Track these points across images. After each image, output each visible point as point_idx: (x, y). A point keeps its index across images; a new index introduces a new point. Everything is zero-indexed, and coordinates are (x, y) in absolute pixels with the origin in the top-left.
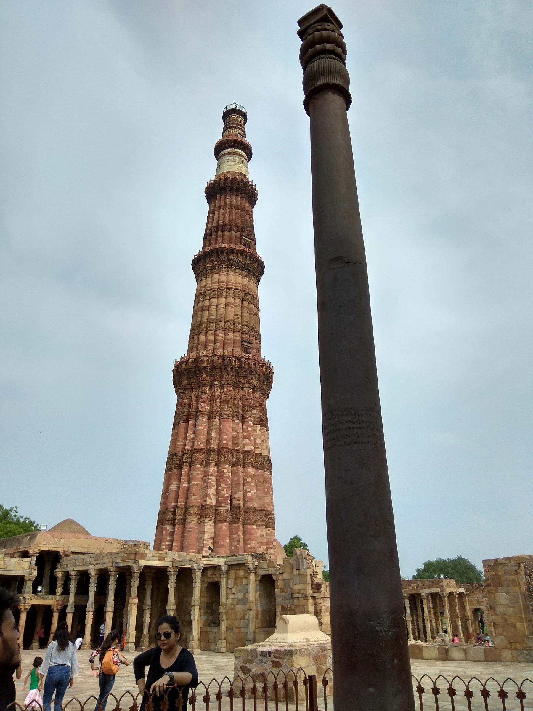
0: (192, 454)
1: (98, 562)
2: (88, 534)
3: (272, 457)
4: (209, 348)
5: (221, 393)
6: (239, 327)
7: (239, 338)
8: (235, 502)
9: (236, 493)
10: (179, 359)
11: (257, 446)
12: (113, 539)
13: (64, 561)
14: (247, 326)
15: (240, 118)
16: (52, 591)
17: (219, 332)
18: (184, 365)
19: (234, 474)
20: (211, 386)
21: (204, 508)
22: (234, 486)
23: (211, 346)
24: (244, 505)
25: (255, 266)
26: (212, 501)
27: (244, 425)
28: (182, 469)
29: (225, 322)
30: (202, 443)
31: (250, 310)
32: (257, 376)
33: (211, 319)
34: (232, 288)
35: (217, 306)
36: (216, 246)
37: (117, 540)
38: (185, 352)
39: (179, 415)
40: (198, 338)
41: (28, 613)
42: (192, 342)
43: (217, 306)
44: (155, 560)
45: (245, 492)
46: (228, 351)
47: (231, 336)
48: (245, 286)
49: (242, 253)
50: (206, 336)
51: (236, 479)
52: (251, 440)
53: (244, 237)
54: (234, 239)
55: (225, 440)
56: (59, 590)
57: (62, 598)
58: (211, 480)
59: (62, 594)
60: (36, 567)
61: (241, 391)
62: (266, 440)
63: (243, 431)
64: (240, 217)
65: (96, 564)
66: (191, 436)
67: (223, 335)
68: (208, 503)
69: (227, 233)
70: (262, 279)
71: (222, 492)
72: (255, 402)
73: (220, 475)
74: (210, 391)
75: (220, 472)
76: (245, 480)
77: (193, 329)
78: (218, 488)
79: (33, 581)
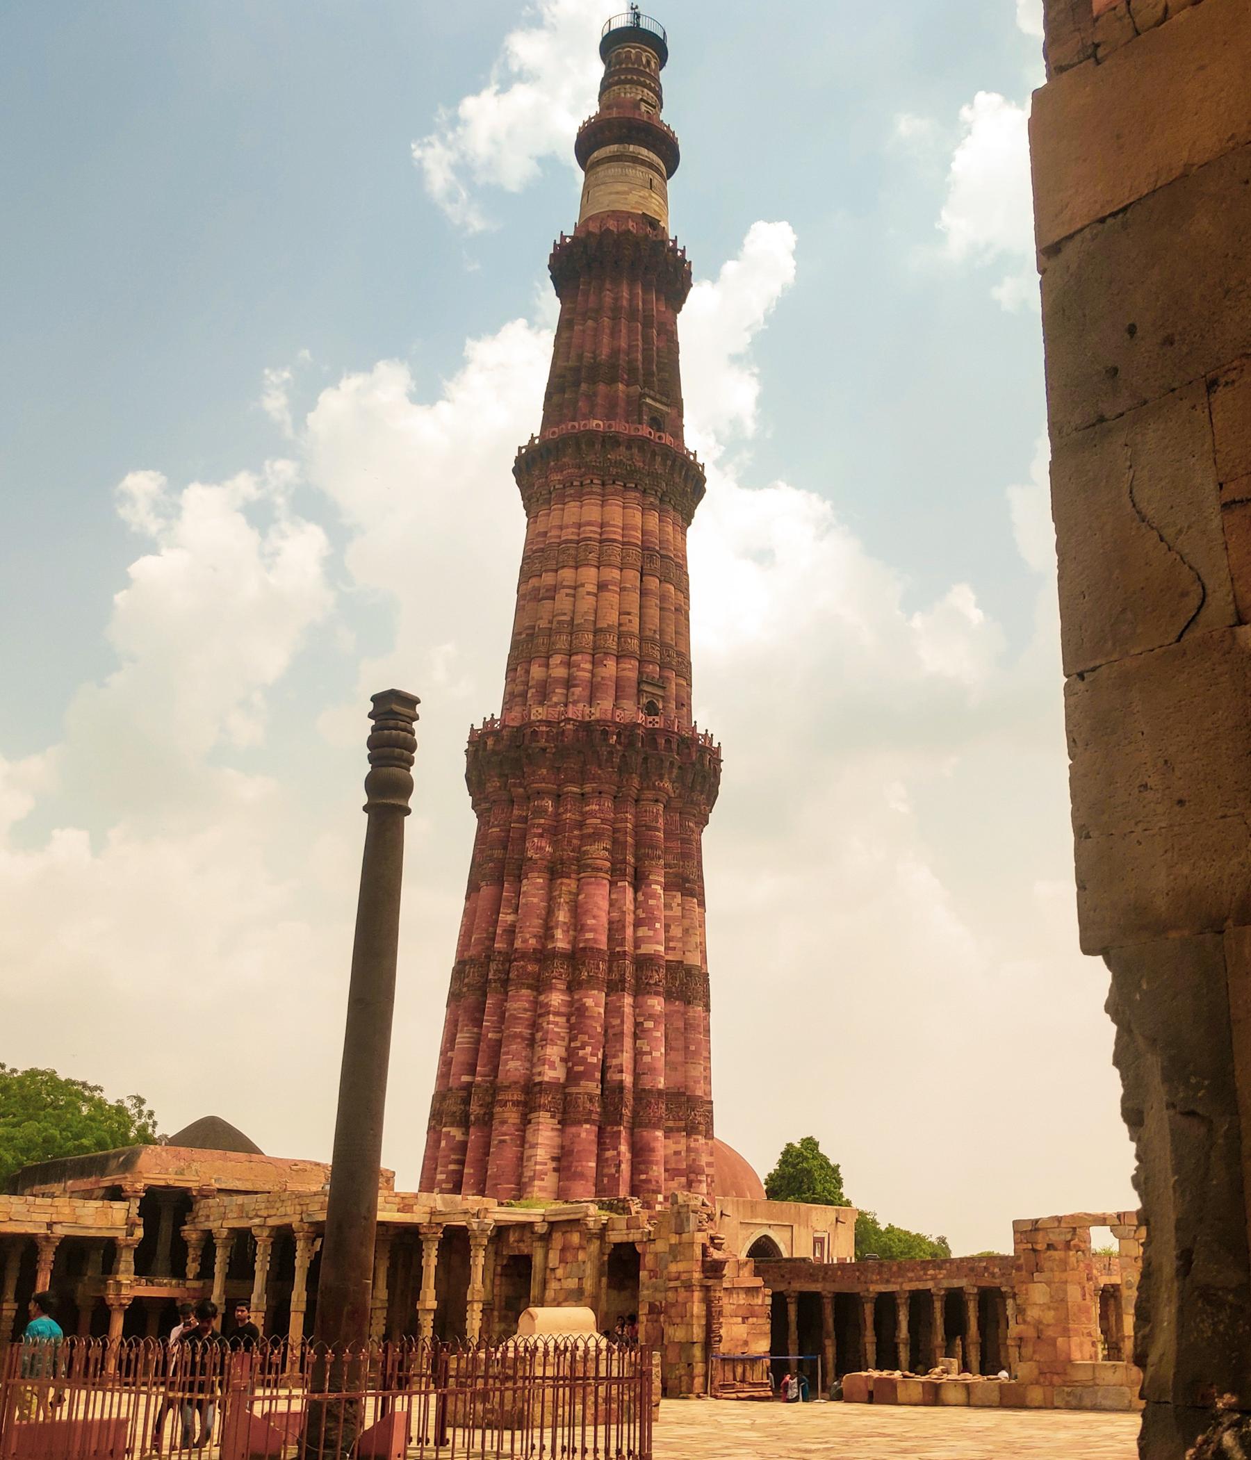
0: (511, 962)
1: (272, 1212)
2: (257, 1151)
3: (712, 969)
4: (555, 699)
5: (583, 814)
6: (634, 644)
7: (634, 675)
8: (613, 1076)
9: (615, 1056)
10: (479, 726)
11: (671, 944)
12: (311, 1163)
13: (202, 1207)
14: (653, 640)
15: (648, 54)
16: (178, 1272)
17: (579, 657)
18: (490, 742)
19: (612, 1010)
20: (558, 798)
21: (537, 1089)
22: (611, 1038)
23: (558, 695)
24: (635, 1084)
25: (677, 480)
26: (553, 1073)
27: (640, 894)
28: (485, 995)
29: (597, 632)
30: (535, 936)
31: (663, 598)
32: (675, 771)
33: (559, 622)
34: (615, 541)
35: (575, 588)
36: (573, 427)
37: (318, 1164)
38: (494, 708)
39: (480, 865)
40: (528, 672)
41: (126, 1313)
42: (513, 680)
43: (575, 588)
44: (390, 1211)
45: (638, 1054)
46: (604, 707)
47: (610, 668)
48: (650, 533)
49: (643, 443)
50: (547, 666)
51: (617, 1022)
52: (655, 930)
53: (648, 400)
54: (622, 404)
55: (591, 930)
56: (192, 1268)
57: (196, 1284)
58: (556, 1024)
59: (199, 1277)
60: (140, 1221)
61: (633, 810)
62: (691, 928)
63: (636, 908)
64: (640, 344)
65: (269, 1216)
66: (506, 918)
67: (588, 666)
68: (546, 1079)
69: (602, 388)
70: (701, 511)
71: (581, 1053)
72: (669, 835)
73: (576, 1014)
74: (556, 807)
75: (576, 1005)
76: (637, 1025)
77: (515, 645)
78: (572, 1045)
79: (136, 1250)
